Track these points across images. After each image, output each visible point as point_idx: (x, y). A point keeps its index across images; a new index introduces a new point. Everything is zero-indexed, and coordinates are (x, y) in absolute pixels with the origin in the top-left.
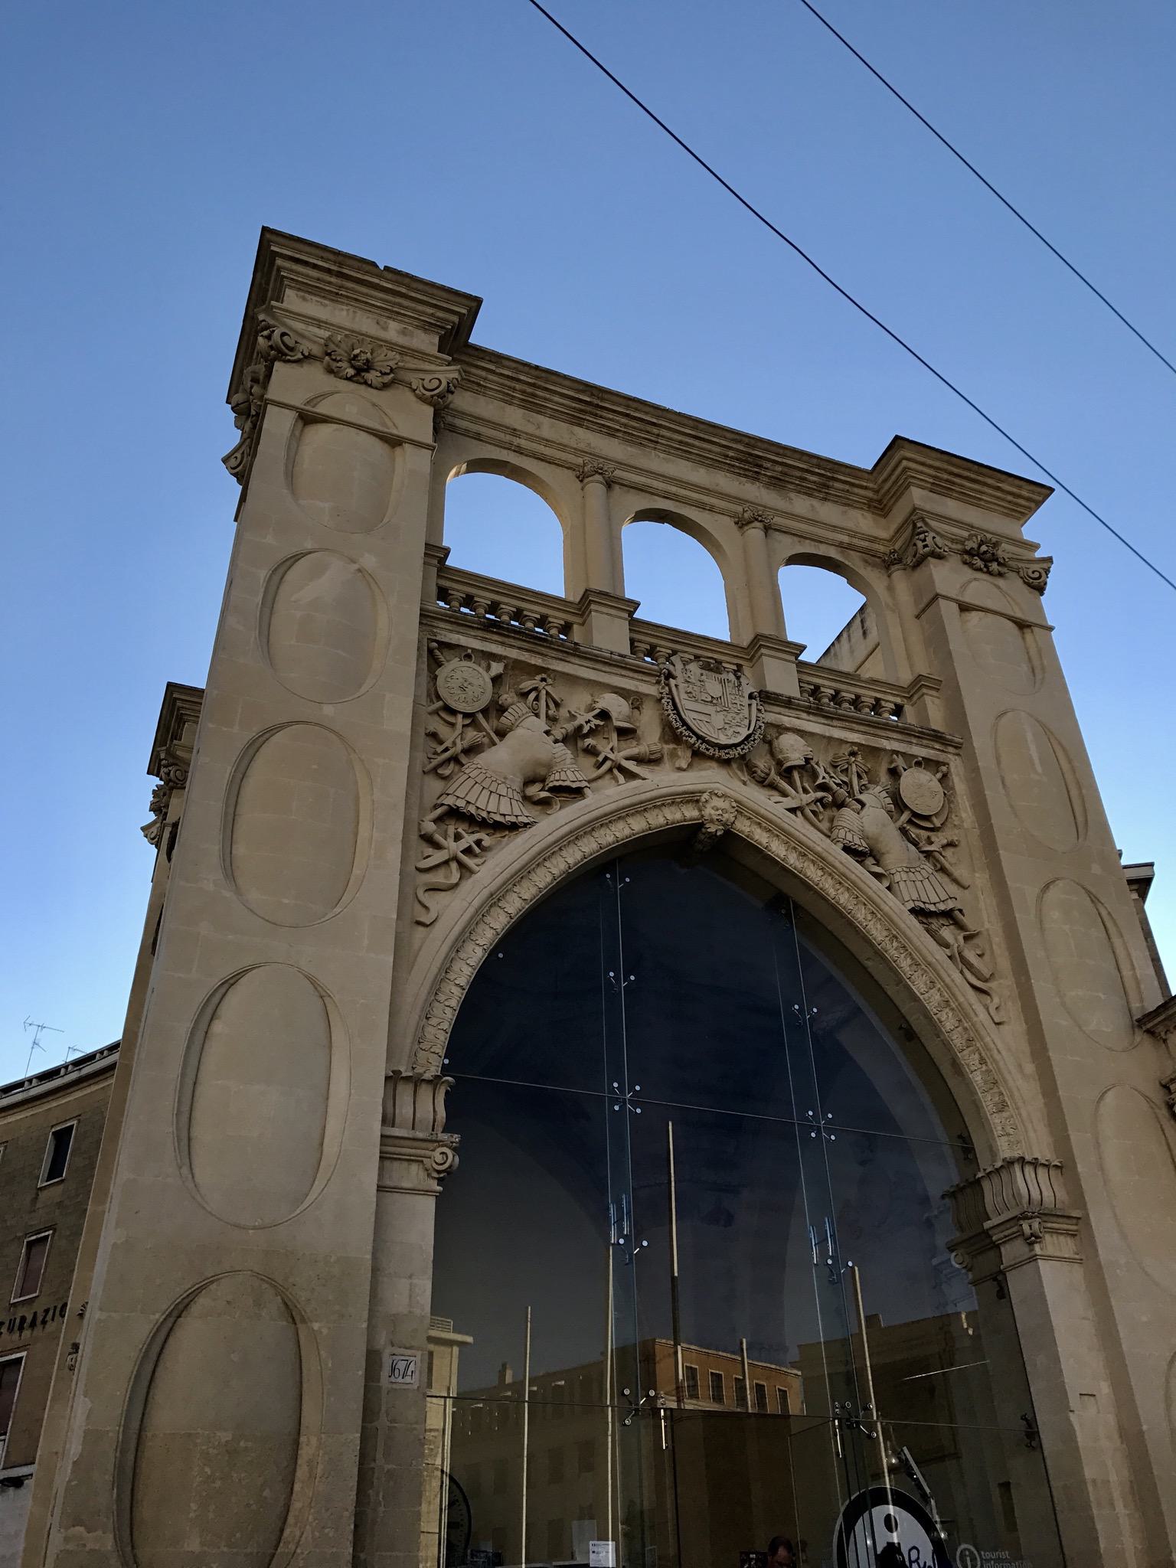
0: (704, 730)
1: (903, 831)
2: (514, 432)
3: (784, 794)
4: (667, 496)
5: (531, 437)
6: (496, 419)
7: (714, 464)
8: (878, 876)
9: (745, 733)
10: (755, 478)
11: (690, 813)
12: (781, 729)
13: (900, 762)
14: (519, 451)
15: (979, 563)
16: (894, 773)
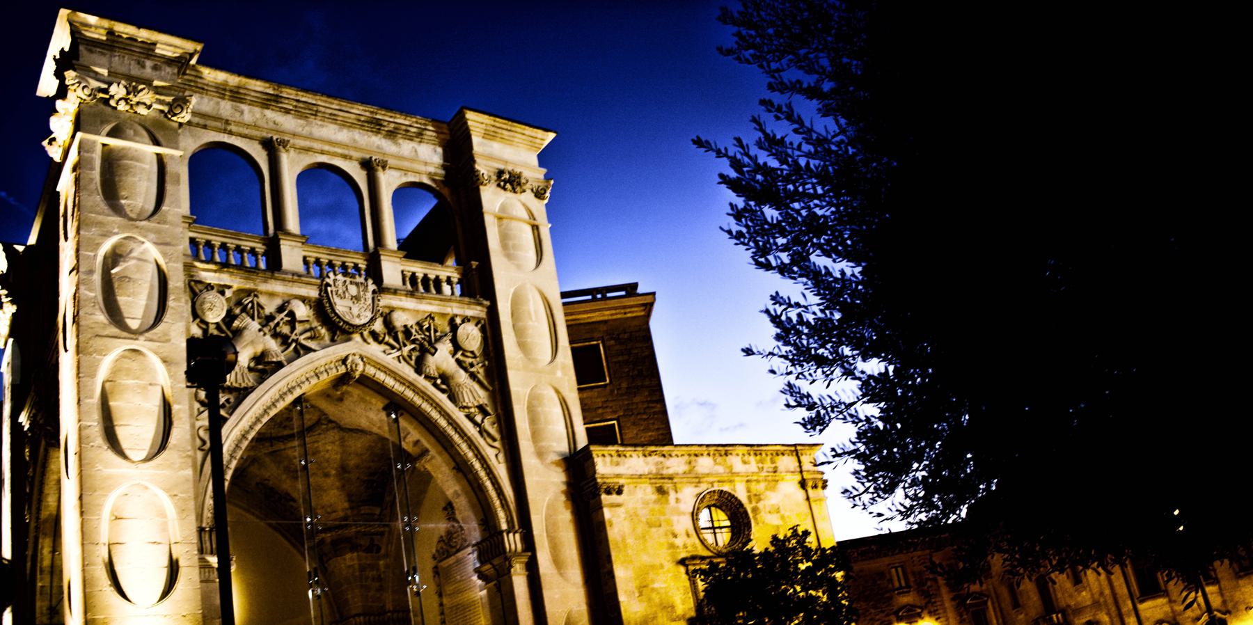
0: (347, 318)
1: (458, 361)
2: (227, 122)
3: (393, 347)
4: (322, 152)
5: (238, 123)
6: (214, 114)
7: (351, 126)
8: (443, 391)
9: (369, 315)
10: (378, 132)
11: (342, 370)
12: (392, 310)
13: (458, 321)
14: (231, 133)
15: (508, 186)
16: (454, 328)
